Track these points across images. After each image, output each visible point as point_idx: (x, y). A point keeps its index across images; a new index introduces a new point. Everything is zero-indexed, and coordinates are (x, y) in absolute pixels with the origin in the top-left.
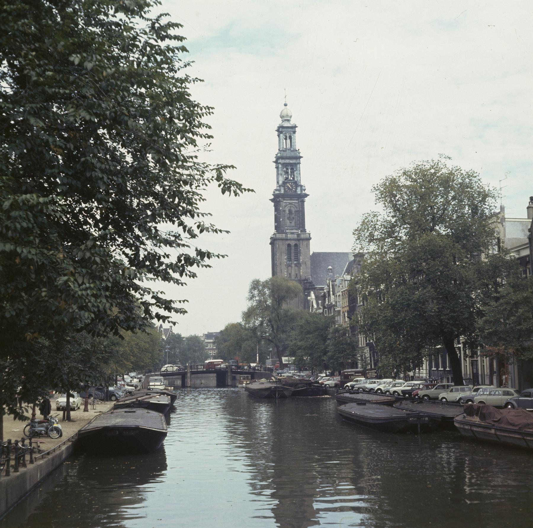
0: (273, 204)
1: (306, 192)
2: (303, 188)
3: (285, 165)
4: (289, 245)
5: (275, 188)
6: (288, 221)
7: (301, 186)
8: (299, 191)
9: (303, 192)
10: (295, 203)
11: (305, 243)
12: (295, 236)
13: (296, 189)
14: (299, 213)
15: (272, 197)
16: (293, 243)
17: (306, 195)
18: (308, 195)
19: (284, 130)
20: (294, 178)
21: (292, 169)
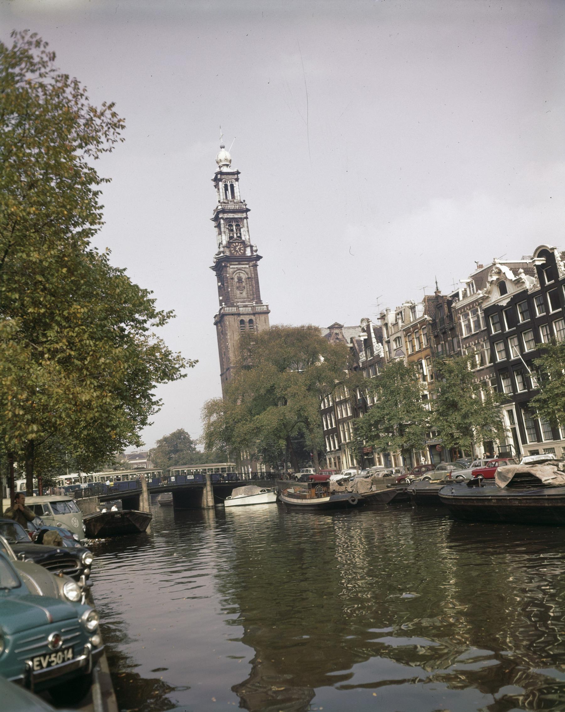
0: (215, 273)
1: (259, 253)
2: (254, 249)
3: (229, 221)
4: (242, 322)
5: (217, 251)
6: (238, 292)
7: (251, 247)
8: (248, 253)
9: (255, 254)
10: (245, 268)
11: (262, 317)
12: (249, 310)
13: (245, 251)
14: (252, 281)
15: (214, 265)
16: (246, 319)
17: (259, 258)
18: (261, 257)
19: (223, 177)
20: (240, 237)
21: (237, 225)
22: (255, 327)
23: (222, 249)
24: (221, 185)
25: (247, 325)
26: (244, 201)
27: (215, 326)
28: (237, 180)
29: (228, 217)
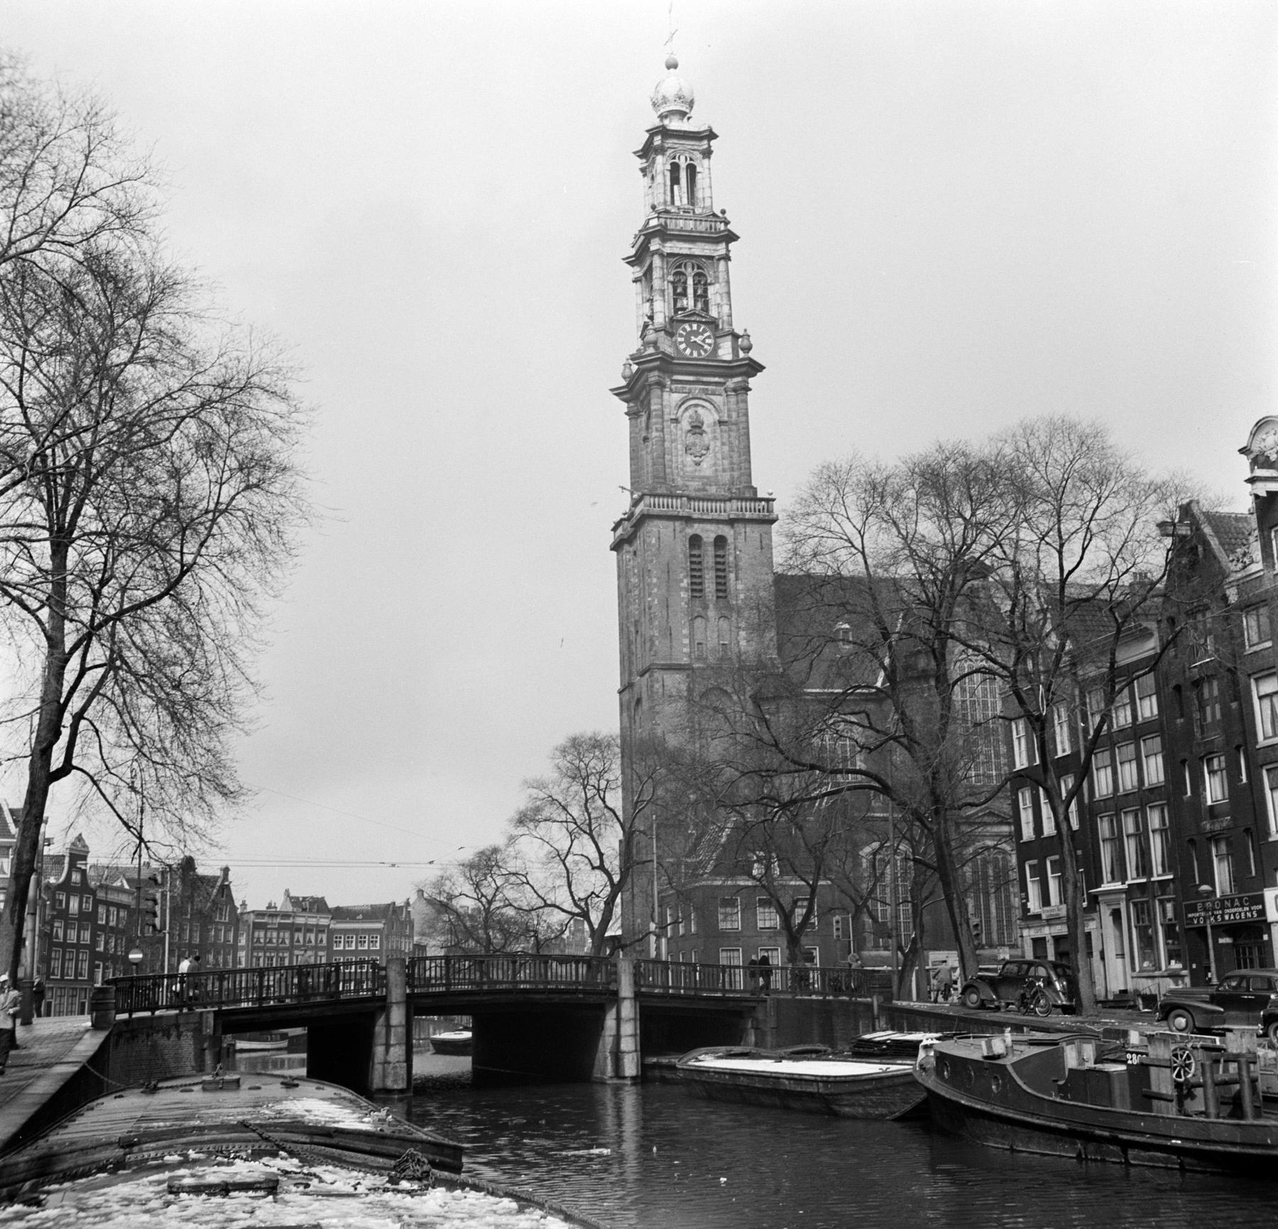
4: (695, 541)
6: (689, 459)
7: (736, 337)
8: (725, 352)
13: (716, 347)
15: (624, 383)
16: (709, 533)
17: (754, 368)
19: (670, 142)
22: (731, 559)
23: (651, 336)
24: (662, 163)
25: (710, 551)
26: (723, 212)
27: (614, 553)
28: (707, 153)
29: (676, 251)
